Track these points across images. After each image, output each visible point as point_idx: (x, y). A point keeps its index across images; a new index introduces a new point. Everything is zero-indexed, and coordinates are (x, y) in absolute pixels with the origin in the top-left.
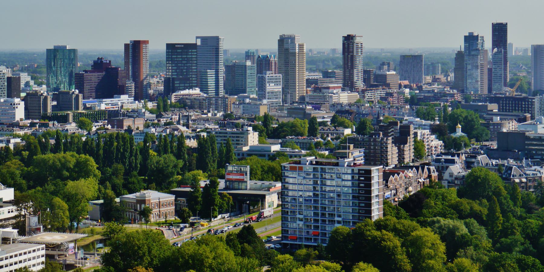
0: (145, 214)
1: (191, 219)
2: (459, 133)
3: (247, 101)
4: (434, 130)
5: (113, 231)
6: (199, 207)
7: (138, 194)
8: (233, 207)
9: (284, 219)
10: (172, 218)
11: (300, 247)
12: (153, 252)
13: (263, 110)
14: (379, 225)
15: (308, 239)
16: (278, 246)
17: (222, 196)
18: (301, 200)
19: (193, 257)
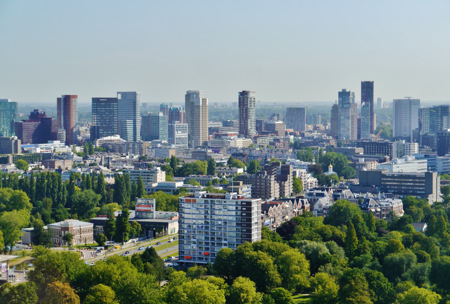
0: (67, 239)
1: (106, 243)
2: (331, 171)
3: (159, 145)
4: (311, 170)
5: (40, 253)
6: (113, 233)
7: (62, 222)
8: (141, 233)
9: (181, 243)
10: (91, 242)
11: (192, 265)
12: (71, 270)
13: (172, 153)
14: (256, 247)
15: (200, 259)
16: (176, 264)
17: (132, 224)
18: (195, 226)
19: (103, 274)
